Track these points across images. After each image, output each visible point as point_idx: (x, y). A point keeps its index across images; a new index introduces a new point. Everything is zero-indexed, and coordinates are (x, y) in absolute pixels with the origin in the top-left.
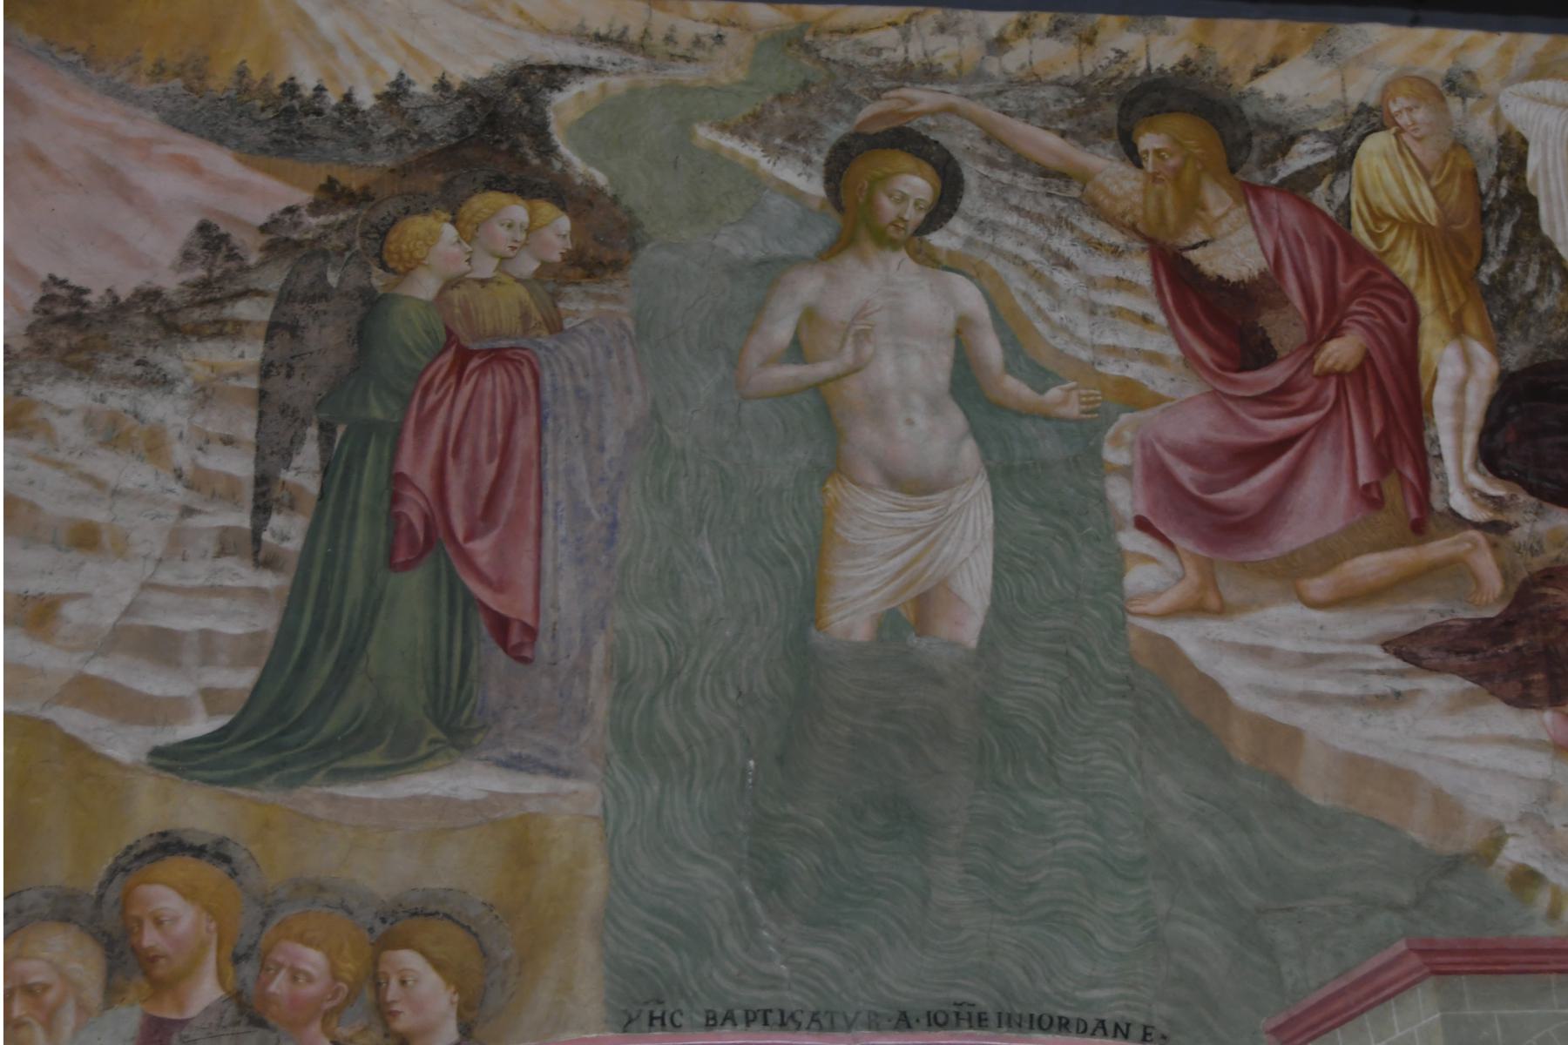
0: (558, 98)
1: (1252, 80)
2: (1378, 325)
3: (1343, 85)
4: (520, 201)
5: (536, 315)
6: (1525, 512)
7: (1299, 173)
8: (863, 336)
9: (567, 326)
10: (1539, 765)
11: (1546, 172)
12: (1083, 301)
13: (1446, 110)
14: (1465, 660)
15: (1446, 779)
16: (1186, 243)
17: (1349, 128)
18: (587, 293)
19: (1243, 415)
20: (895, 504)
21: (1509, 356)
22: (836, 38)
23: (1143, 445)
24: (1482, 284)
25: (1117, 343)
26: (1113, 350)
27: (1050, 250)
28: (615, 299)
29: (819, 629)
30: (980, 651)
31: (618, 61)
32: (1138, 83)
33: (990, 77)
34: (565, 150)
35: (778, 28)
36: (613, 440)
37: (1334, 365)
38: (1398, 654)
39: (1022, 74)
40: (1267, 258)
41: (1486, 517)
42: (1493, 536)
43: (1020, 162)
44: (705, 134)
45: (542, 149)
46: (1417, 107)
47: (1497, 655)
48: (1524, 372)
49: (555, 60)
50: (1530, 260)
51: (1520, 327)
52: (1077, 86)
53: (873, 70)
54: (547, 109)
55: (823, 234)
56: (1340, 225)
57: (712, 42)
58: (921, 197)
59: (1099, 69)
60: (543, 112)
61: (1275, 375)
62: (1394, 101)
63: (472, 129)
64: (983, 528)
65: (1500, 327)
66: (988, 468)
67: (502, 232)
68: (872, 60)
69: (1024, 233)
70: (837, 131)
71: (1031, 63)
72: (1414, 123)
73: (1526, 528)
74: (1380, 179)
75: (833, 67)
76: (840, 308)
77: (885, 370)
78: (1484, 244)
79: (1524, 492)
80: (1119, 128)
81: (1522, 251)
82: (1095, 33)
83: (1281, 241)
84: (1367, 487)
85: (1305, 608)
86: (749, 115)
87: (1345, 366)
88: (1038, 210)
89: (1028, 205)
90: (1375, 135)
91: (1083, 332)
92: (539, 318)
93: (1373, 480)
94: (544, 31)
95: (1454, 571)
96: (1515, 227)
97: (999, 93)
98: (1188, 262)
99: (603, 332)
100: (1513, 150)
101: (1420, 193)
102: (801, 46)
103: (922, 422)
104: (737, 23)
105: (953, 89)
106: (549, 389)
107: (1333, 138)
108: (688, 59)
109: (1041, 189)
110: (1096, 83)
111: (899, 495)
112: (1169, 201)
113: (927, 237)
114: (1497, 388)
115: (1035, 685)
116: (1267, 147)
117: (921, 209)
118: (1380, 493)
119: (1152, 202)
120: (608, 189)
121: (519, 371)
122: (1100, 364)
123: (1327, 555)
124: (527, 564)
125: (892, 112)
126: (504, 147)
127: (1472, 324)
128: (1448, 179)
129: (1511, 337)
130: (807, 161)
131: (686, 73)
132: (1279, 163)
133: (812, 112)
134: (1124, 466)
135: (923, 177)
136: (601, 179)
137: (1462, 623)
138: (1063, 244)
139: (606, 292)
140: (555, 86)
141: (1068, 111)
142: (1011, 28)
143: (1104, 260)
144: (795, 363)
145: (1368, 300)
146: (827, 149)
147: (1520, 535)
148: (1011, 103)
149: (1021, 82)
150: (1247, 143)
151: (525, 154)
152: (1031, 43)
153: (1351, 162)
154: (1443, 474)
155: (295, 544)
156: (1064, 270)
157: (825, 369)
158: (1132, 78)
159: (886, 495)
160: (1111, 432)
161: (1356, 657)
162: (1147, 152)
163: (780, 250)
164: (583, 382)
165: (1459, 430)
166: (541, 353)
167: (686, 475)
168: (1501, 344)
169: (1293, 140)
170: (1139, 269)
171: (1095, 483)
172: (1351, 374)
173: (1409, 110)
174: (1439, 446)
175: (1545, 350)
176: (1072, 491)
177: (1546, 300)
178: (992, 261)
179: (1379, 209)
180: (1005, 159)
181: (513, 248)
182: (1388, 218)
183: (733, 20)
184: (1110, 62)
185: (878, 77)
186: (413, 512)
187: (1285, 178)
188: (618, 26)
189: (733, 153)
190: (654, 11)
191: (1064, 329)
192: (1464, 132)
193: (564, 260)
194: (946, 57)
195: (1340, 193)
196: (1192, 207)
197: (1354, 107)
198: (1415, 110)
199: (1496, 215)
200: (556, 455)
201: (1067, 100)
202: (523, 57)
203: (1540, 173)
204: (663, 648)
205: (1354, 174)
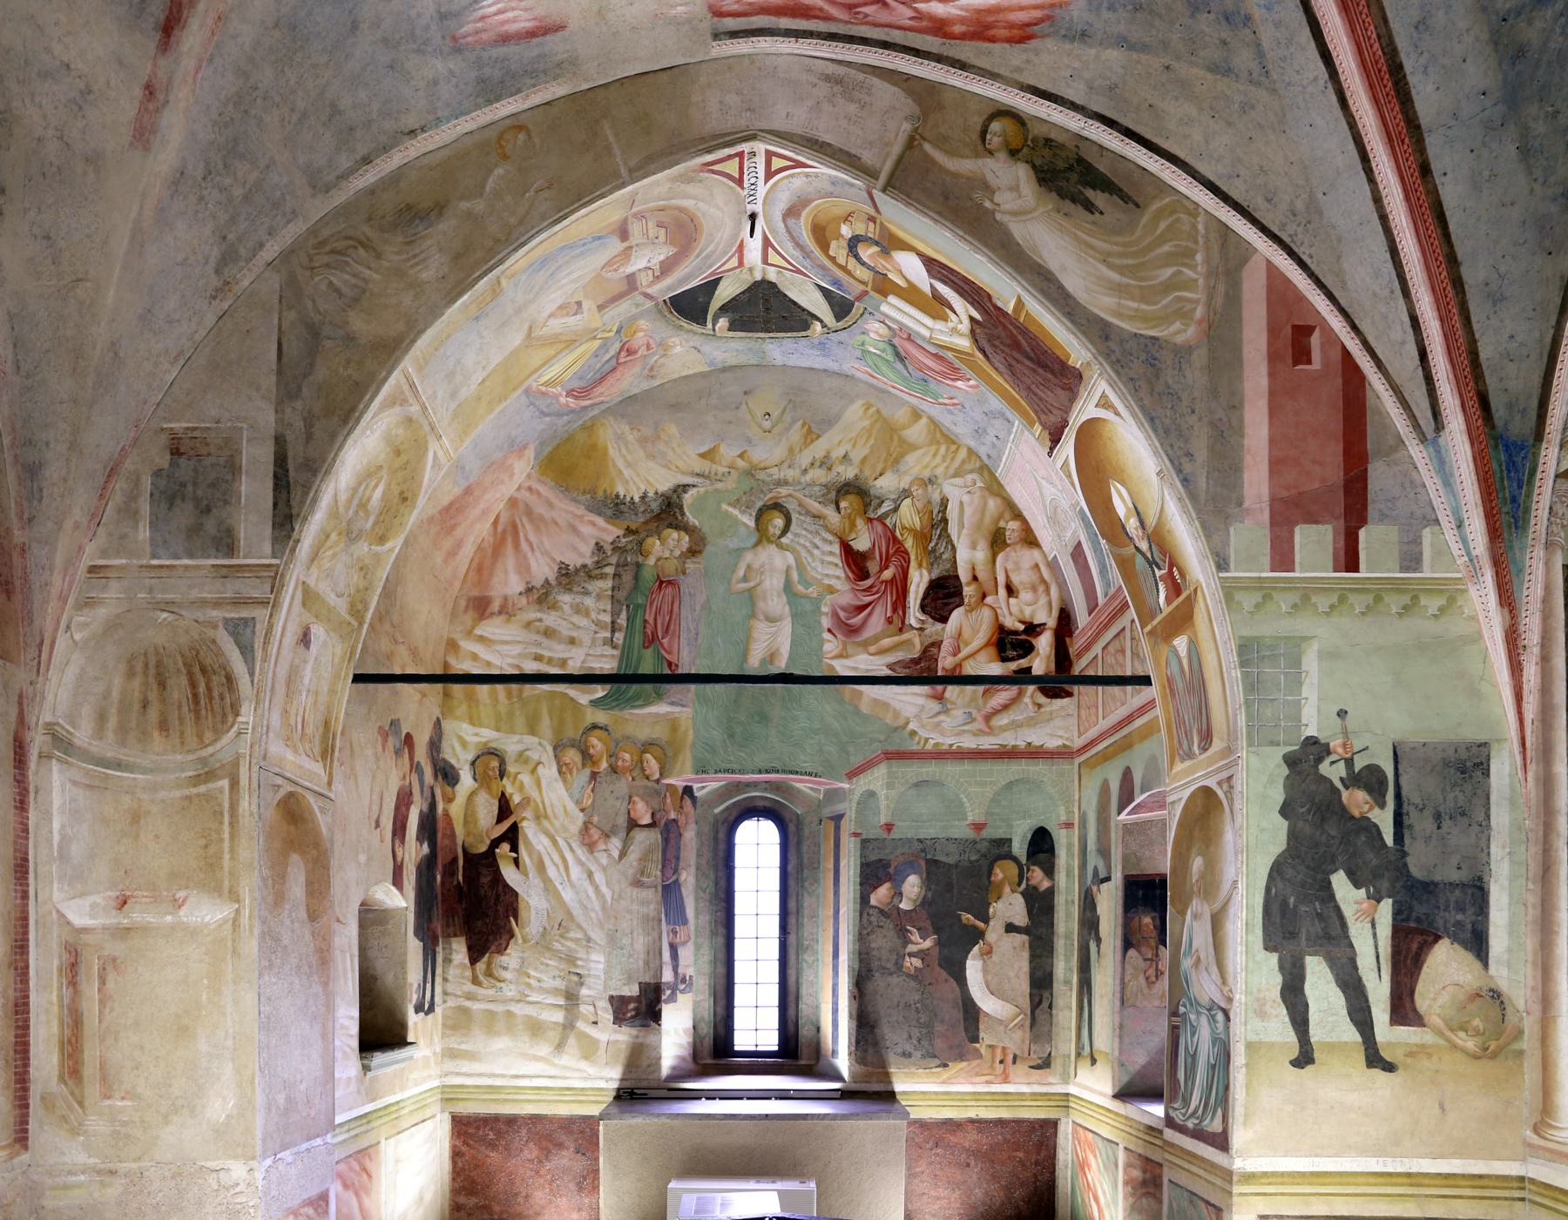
8: (762, 573)
10: (921, 701)
15: (896, 705)
26: (827, 575)
36: (698, 608)
61: (868, 582)
76: (756, 566)
77: (767, 584)
95: (909, 642)
100: (944, 503)
103: (775, 599)
123: (876, 639)
124: (676, 646)
127: (924, 564)
138: (817, 541)
147: (927, 632)
155: (621, 642)
157: (752, 584)
170: (836, 548)
186: (649, 631)
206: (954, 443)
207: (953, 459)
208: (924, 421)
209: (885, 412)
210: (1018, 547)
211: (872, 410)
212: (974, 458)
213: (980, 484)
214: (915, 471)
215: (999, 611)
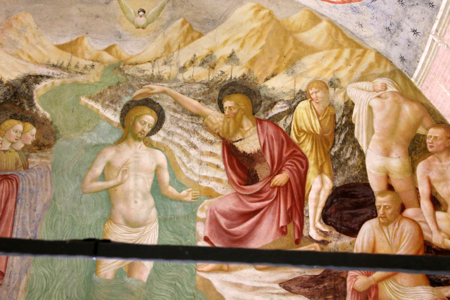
0: (38, 87)
1: (265, 82)
2: (294, 169)
3: (295, 84)
4: (21, 123)
5: (20, 163)
6: (334, 237)
7: (276, 115)
8: (125, 172)
9: (30, 167)
11: (359, 115)
12: (198, 160)
13: (328, 93)
14: (307, 290)
16: (235, 140)
17: (295, 99)
18: (38, 156)
19: (245, 201)
20: (127, 231)
21: (336, 181)
22: (130, 67)
23: (211, 211)
24: (331, 155)
25: (207, 175)
26: (206, 177)
27: (190, 142)
28: (47, 158)
29: (96, 275)
30: (147, 283)
31: (59, 74)
32: (227, 82)
33: (179, 81)
34: (37, 105)
35: (112, 63)
36: (39, 207)
37: (277, 183)
38: (284, 287)
39: (189, 80)
40: (261, 147)
41: (321, 239)
42: (322, 245)
43: (185, 111)
44: (84, 100)
45: (30, 105)
46: (319, 92)
47: (318, 289)
48: (341, 187)
49: (38, 73)
50: (349, 147)
51: (342, 171)
52: (207, 84)
53: (141, 78)
54: (34, 91)
55: (117, 136)
56: (287, 133)
57: (90, 67)
58: (151, 123)
59: (215, 78)
60: (32, 92)
61: (257, 187)
62: (311, 89)
63: (8, 97)
64: (154, 240)
65: (335, 171)
66: (159, 218)
67: (13, 133)
68: (141, 74)
69: (182, 136)
70: (126, 99)
71: (193, 76)
72: (317, 97)
73: (334, 243)
74: (303, 117)
75: (128, 77)
76: (118, 163)
77: (131, 184)
78: (334, 141)
79: (335, 230)
80: (218, 99)
81: (347, 143)
82: (215, 65)
83: (266, 139)
84: (282, 227)
85: (256, 270)
86: (99, 94)
87: (281, 184)
88: (187, 128)
89: (185, 126)
90: (303, 101)
91: (197, 171)
92: (21, 164)
93: (285, 225)
94: (36, 63)
96: (345, 135)
97: (181, 86)
98: (235, 146)
99: (41, 169)
101: (315, 122)
102: (119, 69)
103: (140, 202)
104: (99, 61)
105: (166, 85)
106: (21, 189)
107: (289, 103)
108: (82, 74)
109: (190, 121)
110: (213, 83)
111: (129, 228)
112: (231, 125)
113: (151, 137)
114: (331, 192)
115: (163, 295)
116: (266, 106)
117: (150, 127)
118: (287, 230)
119: (226, 125)
120: (50, 119)
121: (12, 182)
122: (201, 182)
125: (145, 93)
126: (18, 104)
127: (326, 170)
128: (326, 116)
129: (338, 174)
130: (115, 110)
131: (80, 78)
132: (269, 112)
133: (119, 93)
134: (203, 218)
135: (152, 116)
136: (48, 115)
137: (307, 277)
138: (195, 140)
139: (44, 155)
140: (37, 82)
141: (202, 93)
142: (188, 63)
143: (207, 145)
144: (101, 181)
145: (292, 160)
146: (122, 106)
148: (185, 90)
149: (189, 83)
150: (260, 105)
151: (25, 106)
152: (194, 68)
153: (294, 111)
154: (308, 223)
156: (193, 149)
157: (111, 183)
158: (225, 81)
159: (125, 228)
160: (201, 206)
161: (270, 288)
162: (226, 108)
163: (103, 142)
164: (32, 187)
165: (316, 207)
166: (20, 176)
167: (61, 220)
168: (335, 177)
169: (275, 103)
170: (218, 149)
171: (193, 224)
172: (283, 187)
173: (316, 92)
174: (309, 213)
175: (349, 179)
176: (185, 227)
177: (352, 161)
178: (171, 146)
179: (301, 128)
180: (180, 110)
181: (16, 139)
182: (303, 131)
183: (98, 60)
184: (219, 76)
185: (142, 80)
187: (271, 117)
188: (61, 62)
189: (92, 107)
190: (73, 56)
191: (191, 170)
192: (333, 101)
193: (32, 144)
194: (165, 73)
195: (288, 122)
196: (239, 126)
197: (297, 91)
198: (318, 93)
199: (340, 131)
200: (20, 212)
201: (202, 89)
202: (28, 72)
203: (357, 115)
204: (45, 281)
205: (294, 115)
206: (359, 47)
207: (359, 62)
208: (324, 24)
209: (279, 15)
210: (443, 156)
211: (263, 13)
212: (384, 62)
213: (391, 89)
214: (313, 74)
215: (423, 226)
